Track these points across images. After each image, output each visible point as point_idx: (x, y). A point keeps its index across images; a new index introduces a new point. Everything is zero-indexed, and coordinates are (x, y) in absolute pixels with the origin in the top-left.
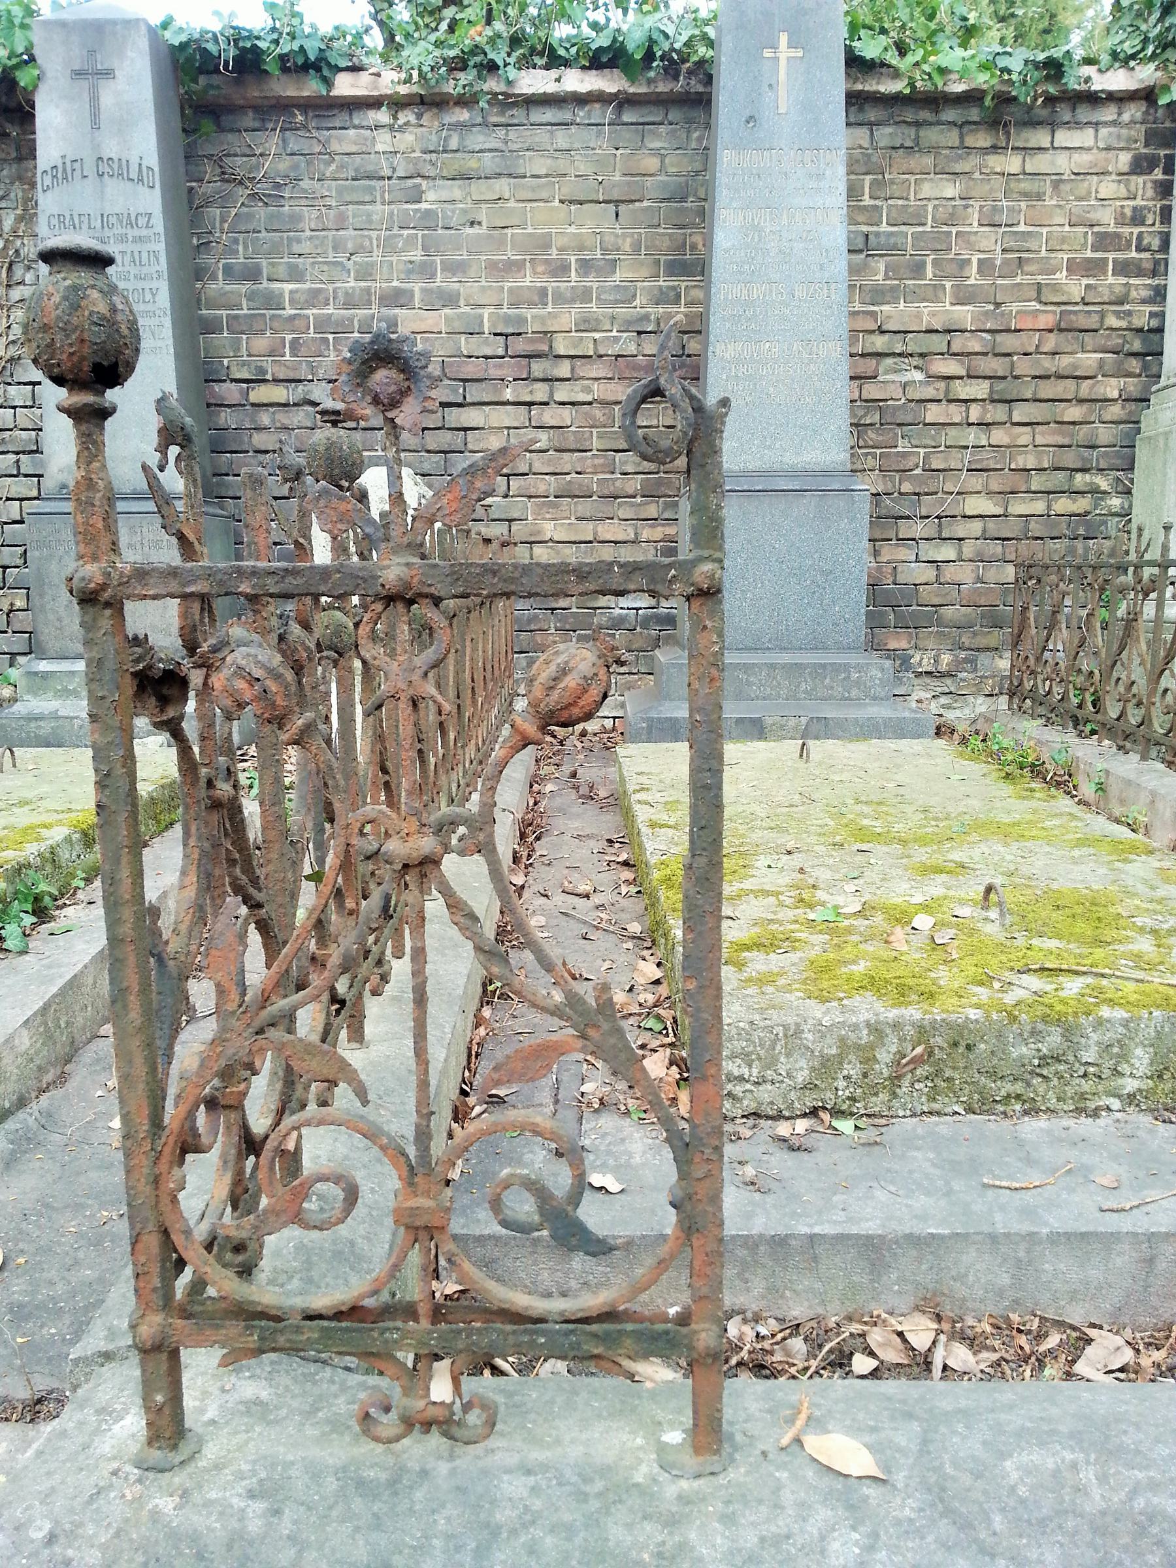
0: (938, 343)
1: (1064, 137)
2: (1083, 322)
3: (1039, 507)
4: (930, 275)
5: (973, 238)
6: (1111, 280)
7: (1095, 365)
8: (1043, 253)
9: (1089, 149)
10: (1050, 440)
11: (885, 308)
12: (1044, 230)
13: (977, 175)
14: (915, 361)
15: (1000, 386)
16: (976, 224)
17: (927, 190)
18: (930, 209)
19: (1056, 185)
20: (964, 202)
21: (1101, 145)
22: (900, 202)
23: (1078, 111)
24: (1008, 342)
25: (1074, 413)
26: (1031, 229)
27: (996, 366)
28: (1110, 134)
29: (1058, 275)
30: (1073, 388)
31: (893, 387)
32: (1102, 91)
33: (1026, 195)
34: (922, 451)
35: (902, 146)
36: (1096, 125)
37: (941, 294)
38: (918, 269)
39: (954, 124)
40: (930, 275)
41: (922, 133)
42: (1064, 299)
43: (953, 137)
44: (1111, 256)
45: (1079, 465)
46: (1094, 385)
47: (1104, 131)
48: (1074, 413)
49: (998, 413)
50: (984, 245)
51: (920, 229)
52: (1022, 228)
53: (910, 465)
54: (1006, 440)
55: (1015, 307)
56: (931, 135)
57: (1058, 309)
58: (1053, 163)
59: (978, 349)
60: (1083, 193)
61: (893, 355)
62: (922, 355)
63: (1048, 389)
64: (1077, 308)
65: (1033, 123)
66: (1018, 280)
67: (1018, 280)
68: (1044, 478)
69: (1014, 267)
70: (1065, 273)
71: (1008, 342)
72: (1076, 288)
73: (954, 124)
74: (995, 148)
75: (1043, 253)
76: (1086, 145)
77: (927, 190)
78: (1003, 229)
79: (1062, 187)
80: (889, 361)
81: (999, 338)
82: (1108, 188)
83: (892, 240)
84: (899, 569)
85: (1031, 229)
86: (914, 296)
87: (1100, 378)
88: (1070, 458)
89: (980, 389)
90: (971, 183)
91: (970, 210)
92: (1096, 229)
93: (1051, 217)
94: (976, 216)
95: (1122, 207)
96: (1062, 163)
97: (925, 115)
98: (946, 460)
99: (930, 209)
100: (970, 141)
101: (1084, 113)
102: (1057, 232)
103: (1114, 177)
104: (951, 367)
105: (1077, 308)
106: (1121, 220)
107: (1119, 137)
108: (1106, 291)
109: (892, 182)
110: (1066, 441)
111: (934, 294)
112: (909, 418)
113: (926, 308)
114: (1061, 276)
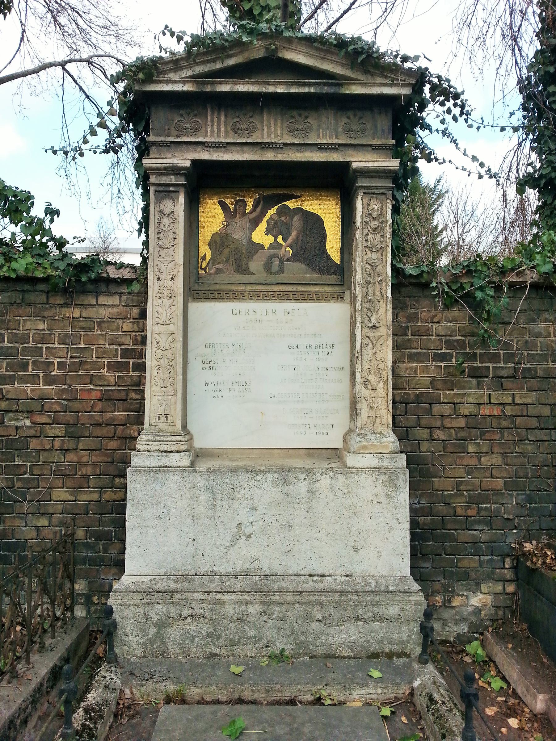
0: (37, 406)
1: (103, 300)
2: (116, 395)
3: (96, 496)
4: (31, 369)
5: (54, 351)
6: (131, 373)
7: (124, 418)
8: (94, 359)
9: (117, 306)
10: (100, 459)
11: (6, 386)
12: (94, 347)
13: (57, 318)
14: (25, 415)
15: (72, 429)
16: (56, 343)
17: (29, 325)
18: (31, 335)
19: (99, 323)
20: (49, 332)
21: (123, 304)
22: (15, 331)
23: (110, 286)
24: (76, 405)
25: (113, 444)
26: (87, 346)
27: (69, 417)
28: (127, 298)
29: (102, 371)
30: (113, 431)
31: (11, 429)
32: (118, 278)
33: (83, 329)
34: (29, 464)
35: (15, 303)
36: (120, 294)
37: (37, 380)
38: (24, 366)
39: (43, 292)
40: (31, 369)
41: (26, 296)
42: (106, 383)
43: (44, 297)
44: (131, 361)
45: (116, 473)
46: (123, 430)
47: (124, 297)
48: (113, 444)
49: (70, 443)
50: (60, 354)
51: (26, 345)
52: (82, 345)
53: (22, 472)
54: (75, 459)
55: (79, 387)
56: (31, 297)
57: (104, 388)
58: (97, 312)
59: (58, 409)
60: (114, 328)
61: (11, 411)
62: (28, 412)
63: (98, 432)
64: (114, 388)
65: (86, 292)
66: (80, 373)
67: (80, 373)
68: (97, 480)
69: (77, 366)
70: (106, 369)
71: (76, 405)
72: (112, 377)
73: (43, 292)
74: (66, 305)
75: (94, 359)
76: (116, 304)
77: (29, 325)
78: (69, 347)
79: (103, 325)
80: (11, 414)
81: (70, 404)
82: (127, 326)
83: (10, 351)
84: (16, 530)
85: (87, 346)
86: (23, 380)
87: (128, 425)
88: (112, 470)
89: (60, 431)
90: (53, 322)
91: (53, 336)
92: (123, 347)
93: (97, 340)
94: (56, 339)
95: (136, 335)
96: (102, 313)
97: (27, 287)
98: (41, 470)
99: (31, 335)
100: (52, 300)
101: (113, 288)
102: (100, 348)
103: (132, 320)
104: (44, 419)
105: (114, 388)
106: (136, 342)
107: (132, 300)
108: (129, 379)
109: (9, 320)
110: (110, 460)
111: (34, 379)
112: (19, 446)
113: (28, 387)
114: (104, 371)
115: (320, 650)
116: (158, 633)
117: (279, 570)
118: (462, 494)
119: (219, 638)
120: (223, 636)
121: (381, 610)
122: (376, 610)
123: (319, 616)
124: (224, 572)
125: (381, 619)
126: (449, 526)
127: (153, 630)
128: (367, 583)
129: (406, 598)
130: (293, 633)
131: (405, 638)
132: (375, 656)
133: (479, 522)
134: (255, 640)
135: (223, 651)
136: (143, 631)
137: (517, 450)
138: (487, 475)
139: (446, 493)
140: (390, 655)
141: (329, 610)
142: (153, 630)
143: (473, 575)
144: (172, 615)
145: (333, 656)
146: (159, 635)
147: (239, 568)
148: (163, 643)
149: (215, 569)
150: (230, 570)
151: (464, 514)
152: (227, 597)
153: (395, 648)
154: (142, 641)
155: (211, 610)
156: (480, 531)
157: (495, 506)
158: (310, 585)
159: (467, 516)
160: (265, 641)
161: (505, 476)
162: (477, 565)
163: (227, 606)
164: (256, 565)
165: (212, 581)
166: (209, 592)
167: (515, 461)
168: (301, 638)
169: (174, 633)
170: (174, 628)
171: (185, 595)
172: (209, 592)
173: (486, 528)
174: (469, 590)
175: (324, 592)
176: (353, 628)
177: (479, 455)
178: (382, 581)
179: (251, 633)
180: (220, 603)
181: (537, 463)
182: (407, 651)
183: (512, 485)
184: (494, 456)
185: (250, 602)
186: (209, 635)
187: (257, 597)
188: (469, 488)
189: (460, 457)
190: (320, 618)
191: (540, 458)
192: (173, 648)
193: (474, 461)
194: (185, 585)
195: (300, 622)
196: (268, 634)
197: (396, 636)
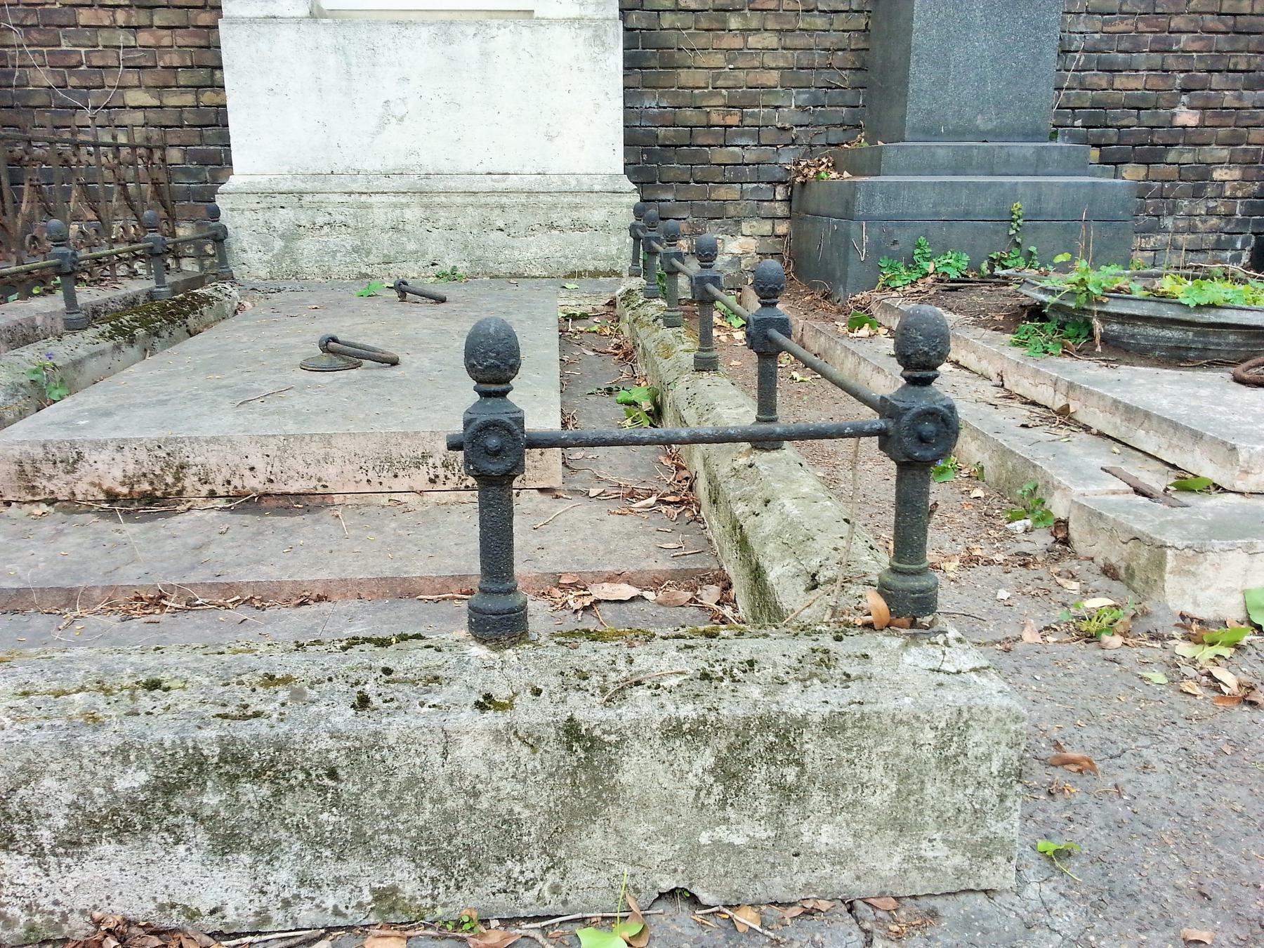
115: (504, 269)
116: (286, 247)
117: (446, 167)
118: (720, 94)
119: (368, 253)
120: (374, 251)
121: (582, 214)
122: (575, 215)
123: (501, 224)
124: (370, 169)
125: (580, 226)
126: (700, 141)
127: (278, 244)
128: (564, 182)
129: (616, 199)
130: (466, 246)
131: (614, 252)
132: (572, 275)
133: (742, 135)
134: (417, 255)
135: (376, 270)
136: (265, 244)
137: (801, 25)
138: (756, 64)
139: (696, 91)
140: (595, 274)
141: (514, 215)
142: (278, 244)
143: (731, 210)
144: (303, 223)
145: (521, 276)
146: (287, 251)
147: (390, 164)
148: (295, 261)
149: (358, 166)
150: (378, 167)
151: (722, 123)
152: (375, 199)
153: (602, 266)
154: (265, 258)
155: (355, 216)
156: (743, 147)
157: (766, 110)
158: (488, 183)
159: (726, 127)
160: (430, 257)
161: (781, 65)
162: (737, 197)
163: (376, 210)
164: (413, 160)
165: (354, 181)
166: (350, 193)
167: (800, 42)
168: (478, 253)
169: (308, 247)
170: (307, 240)
171: (318, 198)
172: (350, 193)
173: (751, 143)
174: (726, 232)
175: (506, 192)
176: (546, 239)
177: (746, 32)
178: (585, 179)
179: (411, 246)
180: (368, 207)
181: (828, 45)
182: (618, 269)
183: (793, 77)
184: (766, 34)
185: (408, 205)
186: (356, 250)
187: (416, 199)
188: (731, 83)
189: (718, 37)
190: (502, 226)
191: (831, 40)
192: (309, 267)
193: (737, 43)
194: (318, 186)
195: (475, 231)
196: (434, 247)
197: (602, 250)
